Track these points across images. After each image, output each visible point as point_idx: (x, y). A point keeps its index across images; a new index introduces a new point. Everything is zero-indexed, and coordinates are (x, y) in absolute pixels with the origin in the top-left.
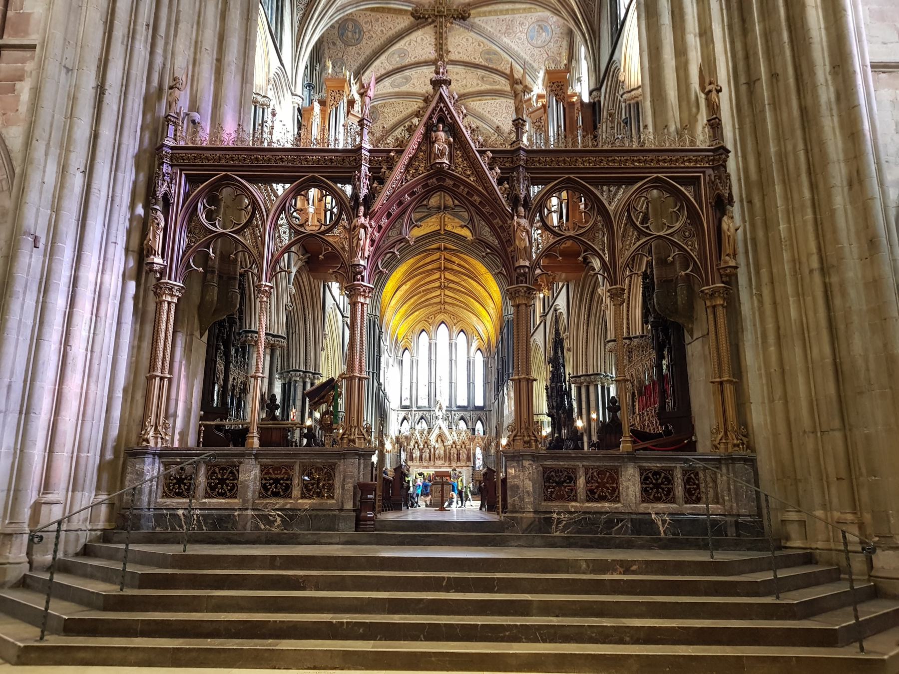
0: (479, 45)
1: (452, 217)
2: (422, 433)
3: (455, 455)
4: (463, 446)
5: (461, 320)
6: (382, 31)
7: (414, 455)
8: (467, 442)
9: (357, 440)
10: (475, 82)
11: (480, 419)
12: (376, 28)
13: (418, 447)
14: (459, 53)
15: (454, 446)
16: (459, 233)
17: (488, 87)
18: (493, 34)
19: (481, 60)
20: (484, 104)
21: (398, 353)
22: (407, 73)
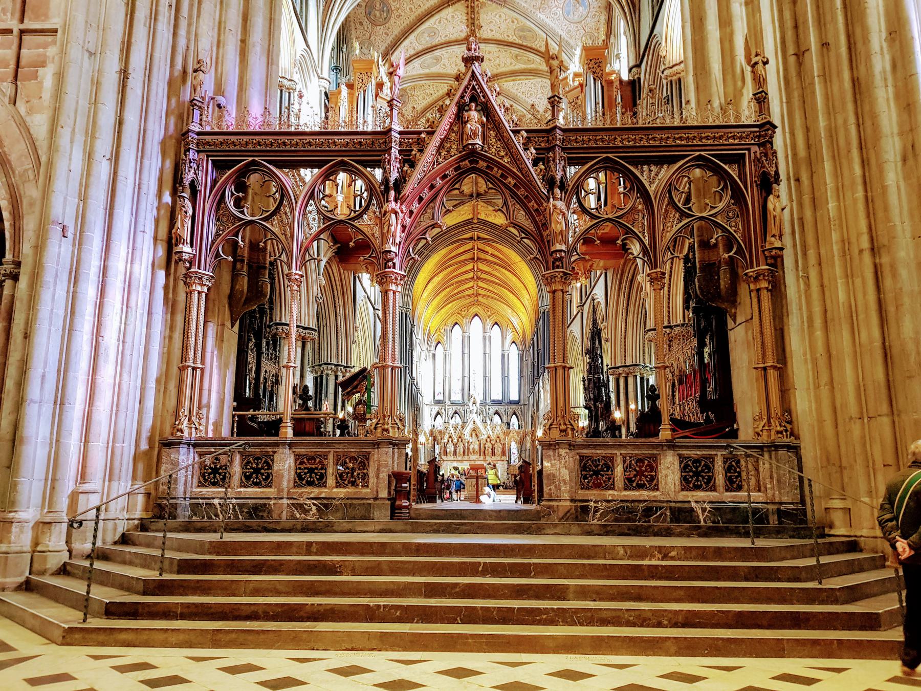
0: (513, 22)
1: (485, 205)
2: (456, 428)
3: (490, 450)
4: (498, 441)
5: (495, 312)
6: (411, 9)
7: (448, 450)
8: (502, 436)
9: (390, 429)
10: (509, 61)
11: (515, 413)
12: (405, 6)
14: (492, 31)
15: (488, 440)
16: (493, 221)
17: (523, 66)
18: (527, 9)
19: (514, 37)
20: (519, 85)
21: (430, 347)
22: (437, 53)
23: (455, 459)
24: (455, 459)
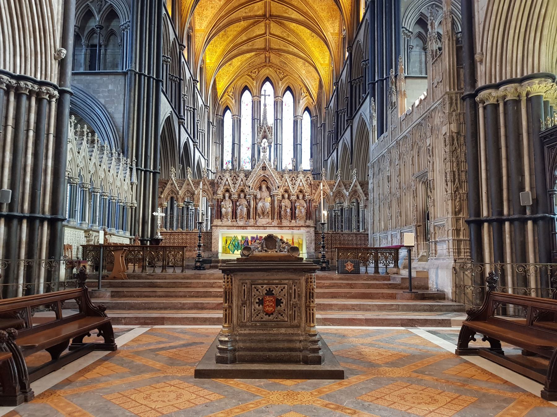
3: (288, 210)
4: (301, 196)
7: (223, 210)
8: (307, 189)
13: (230, 197)
15: (286, 196)
21: (218, 111)
23: (235, 224)
24: (235, 224)
